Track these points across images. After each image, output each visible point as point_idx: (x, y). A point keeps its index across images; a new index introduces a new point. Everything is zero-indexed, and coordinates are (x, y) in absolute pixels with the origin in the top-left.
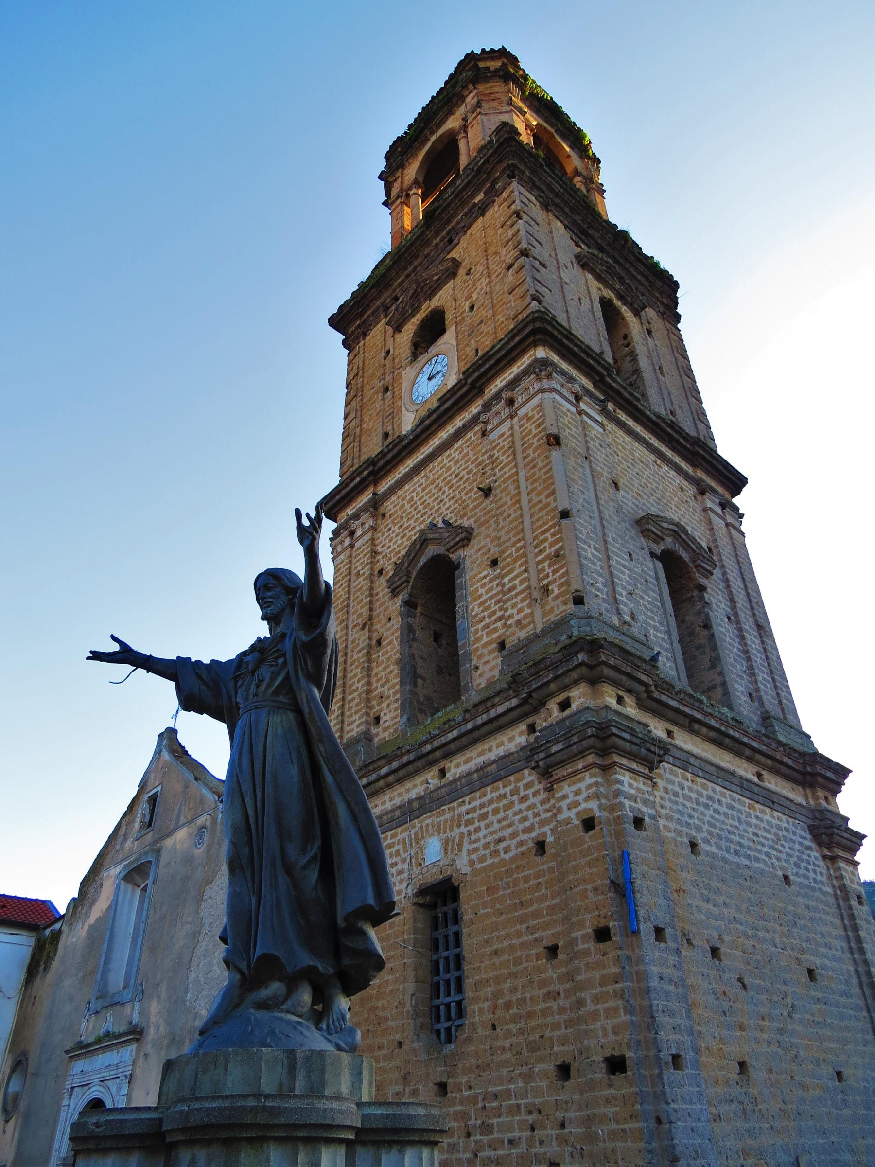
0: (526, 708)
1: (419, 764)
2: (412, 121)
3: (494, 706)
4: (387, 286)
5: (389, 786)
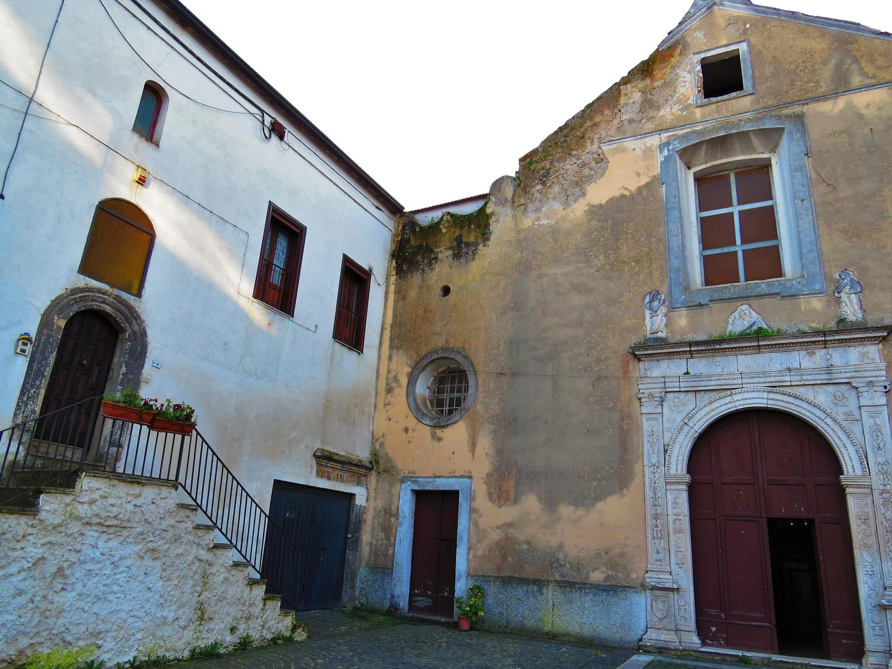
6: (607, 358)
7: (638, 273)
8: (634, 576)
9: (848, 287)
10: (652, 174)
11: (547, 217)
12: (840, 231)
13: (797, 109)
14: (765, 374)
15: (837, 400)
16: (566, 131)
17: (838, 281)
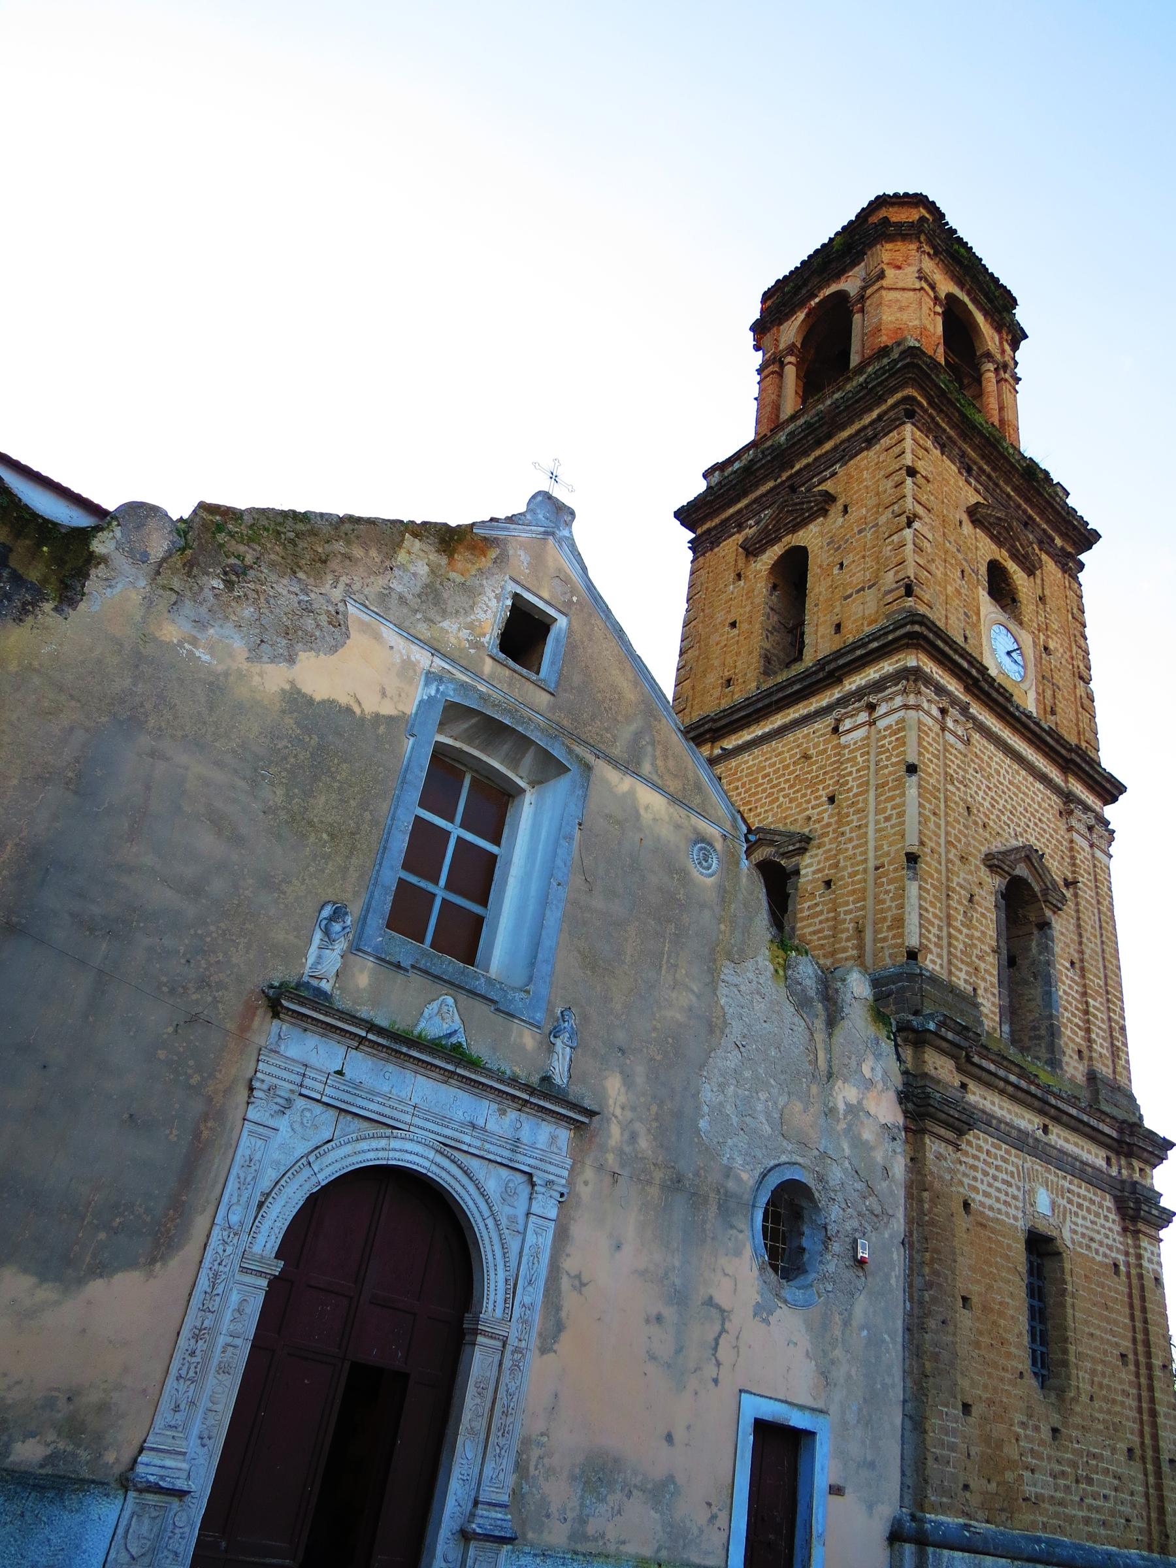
0: (1115, 1145)
1: (1037, 1103)
2: (960, 234)
3: (1103, 1121)
4: (964, 436)
5: (1002, 1092)
6: (221, 986)
7: (327, 857)
8: (110, 1457)
10: (401, 707)
11: (212, 650)
12: (579, 952)
13: (590, 758)
14: (444, 1121)
15: (508, 1194)
16: (300, 527)
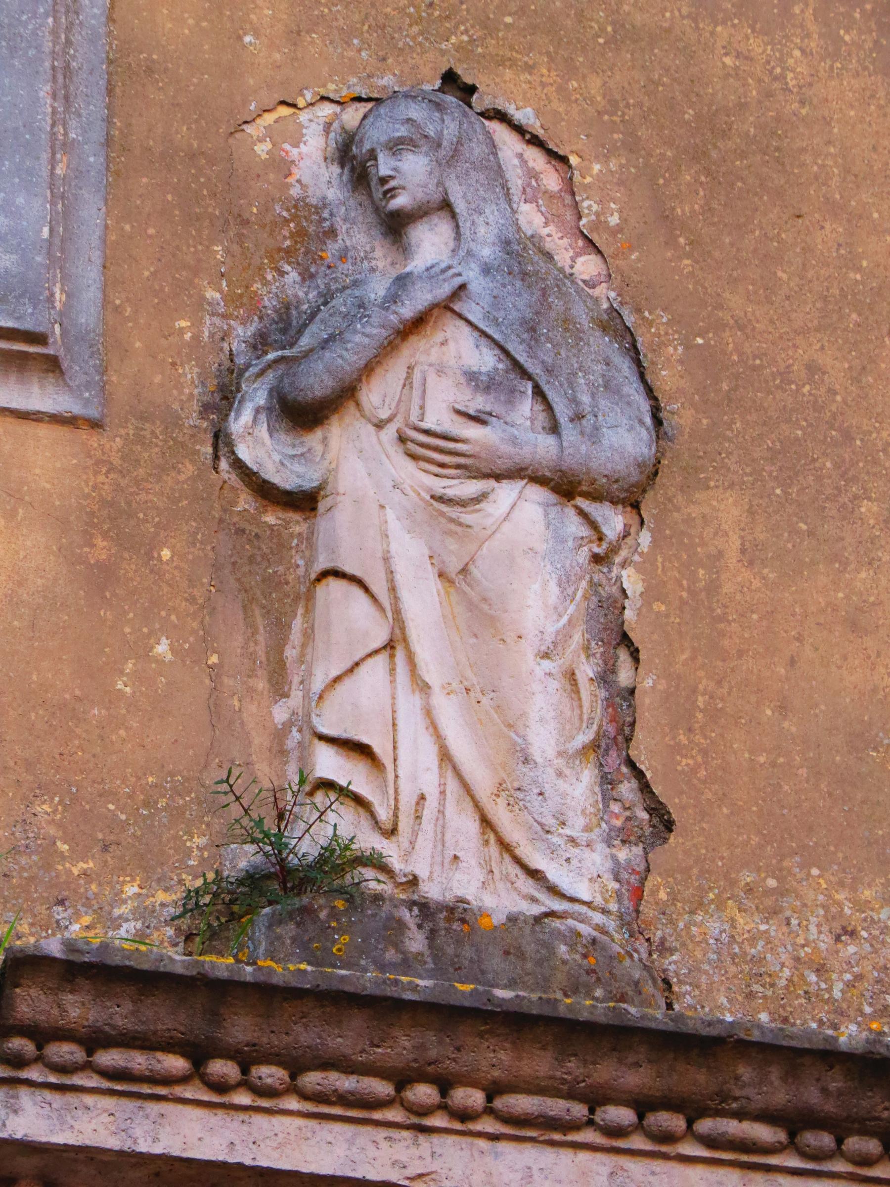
9: (458, 349)
17: (307, 234)
